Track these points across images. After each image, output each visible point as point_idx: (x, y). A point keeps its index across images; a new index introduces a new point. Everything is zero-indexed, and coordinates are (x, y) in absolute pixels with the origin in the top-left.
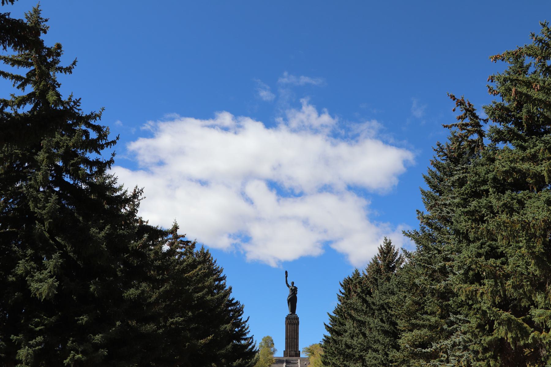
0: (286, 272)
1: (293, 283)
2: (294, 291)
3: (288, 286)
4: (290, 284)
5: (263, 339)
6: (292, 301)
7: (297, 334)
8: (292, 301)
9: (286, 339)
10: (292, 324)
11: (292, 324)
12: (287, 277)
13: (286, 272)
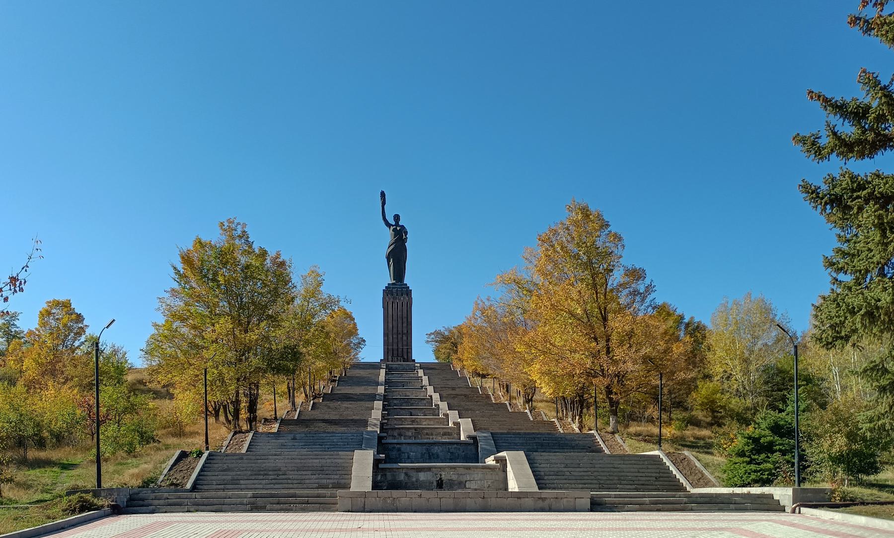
0: (383, 195)
1: (397, 218)
3: (388, 224)
4: (392, 222)
6: (397, 257)
7: (409, 324)
8: (397, 257)
9: (386, 335)
10: (398, 302)
11: (398, 302)
12: (384, 204)
13: (383, 195)
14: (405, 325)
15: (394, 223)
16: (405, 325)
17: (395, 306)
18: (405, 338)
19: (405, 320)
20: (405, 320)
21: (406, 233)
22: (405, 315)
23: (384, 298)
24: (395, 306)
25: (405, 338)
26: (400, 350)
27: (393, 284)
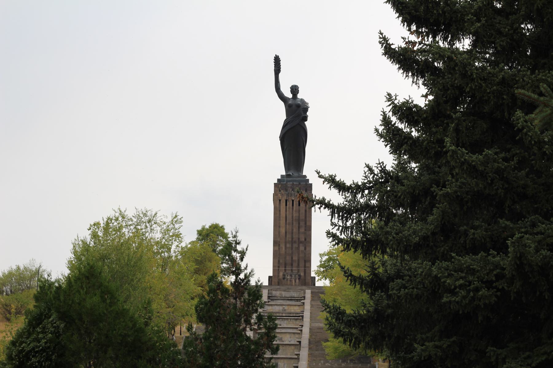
0: (277, 60)
1: (295, 90)
4: (289, 95)
5: (200, 233)
6: (293, 139)
7: (308, 228)
8: (293, 139)
9: (276, 243)
13: (277, 60)
14: (302, 230)
15: (290, 96)
16: (302, 230)
17: (290, 203)
18: (302, 248)
19: (302, 224)
20: (302, 224)
21: (306, 109)
22: (302, 217)
23: (275, 195)
24: (290, 203)
25: (302, 248)
26: (295, 264)
27: (288, 176)
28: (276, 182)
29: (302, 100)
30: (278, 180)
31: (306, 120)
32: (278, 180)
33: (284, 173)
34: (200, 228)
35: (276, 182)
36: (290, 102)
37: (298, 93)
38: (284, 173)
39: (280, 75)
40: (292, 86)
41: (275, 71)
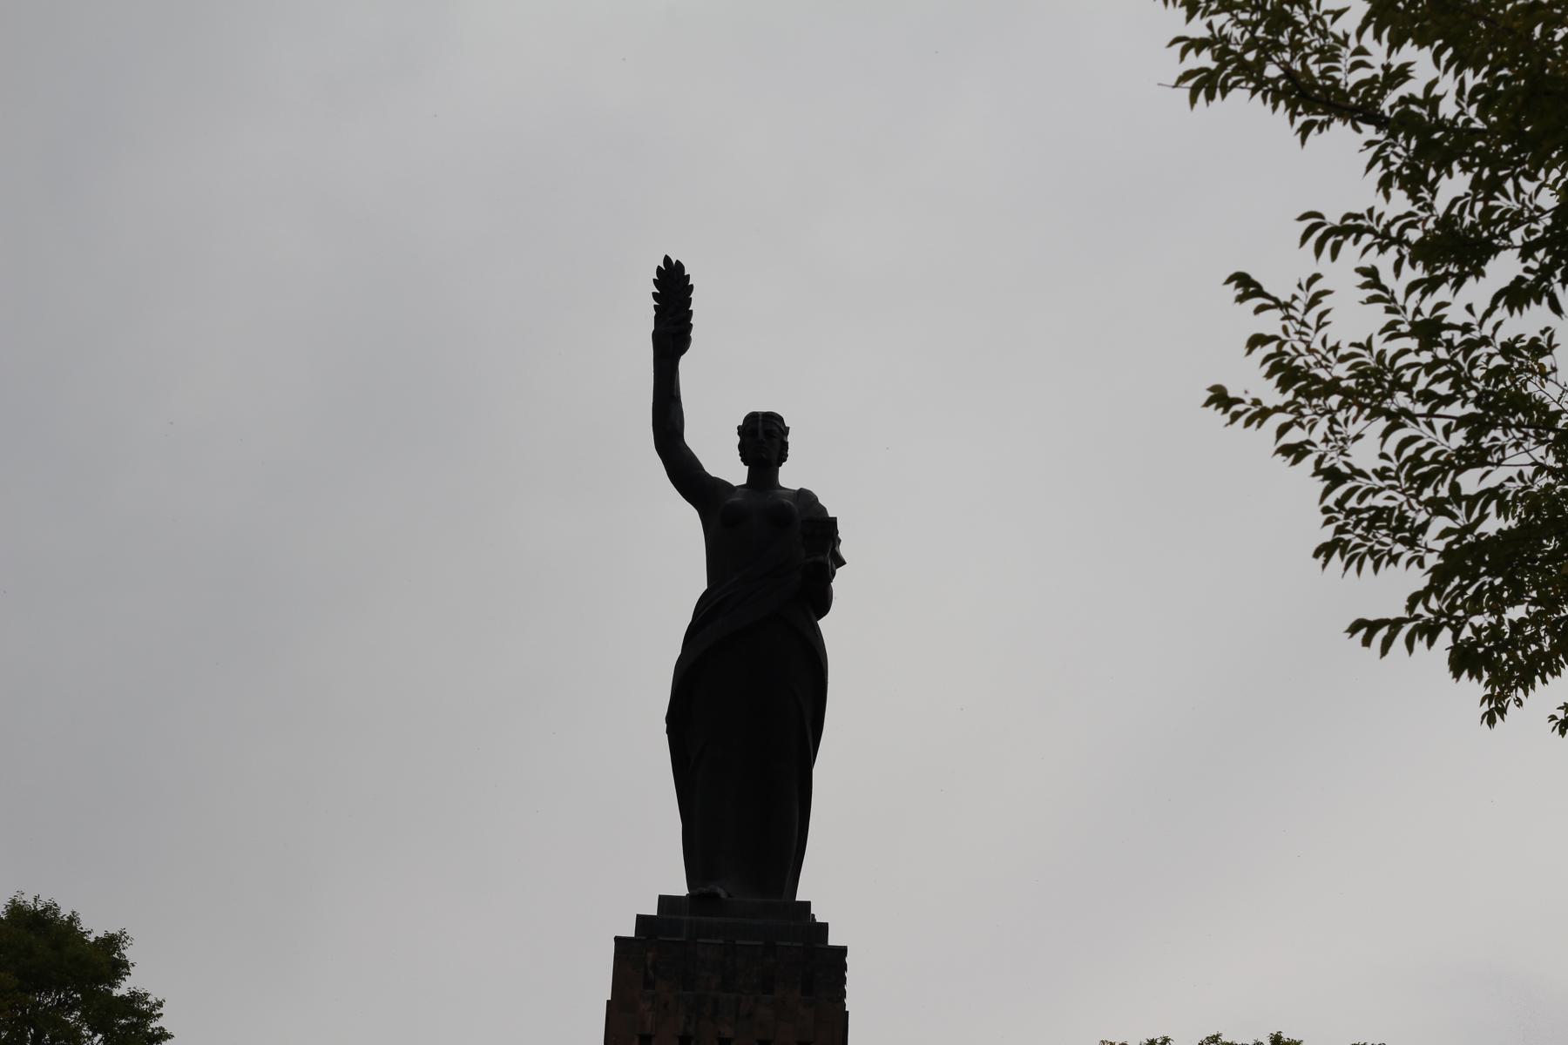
0: (673, 288)
1: (764, 438)
2: (769, 564)
4: (725, 464)
5: (125, 965)
13: (673, 288)
15: (735, 473)
28: (629, 931)
29: (806, 498)
30: (642, 920)
31: (822, 604)
32: (642, 920)
33: (680, 888)
34: (130, 953)
35: (629, 931)
36: (736, 499)
37: (782, 457)
38: (680, 888)
39: (686, 364)
40: (752, 419)
41: (657, 337)
